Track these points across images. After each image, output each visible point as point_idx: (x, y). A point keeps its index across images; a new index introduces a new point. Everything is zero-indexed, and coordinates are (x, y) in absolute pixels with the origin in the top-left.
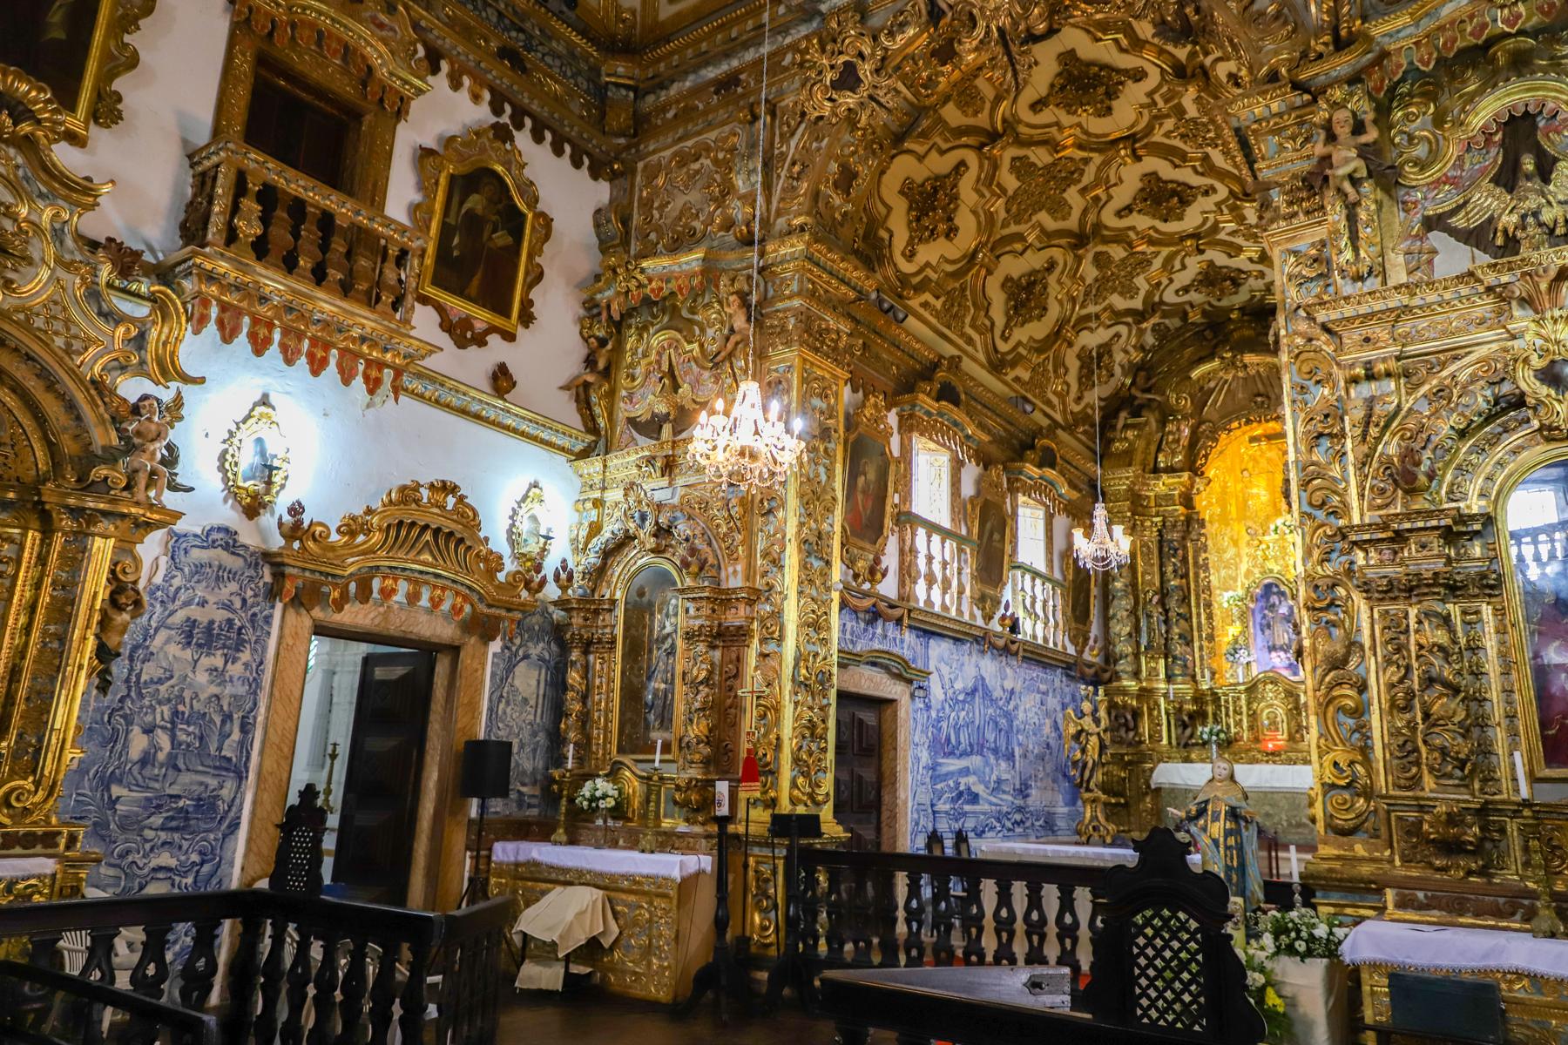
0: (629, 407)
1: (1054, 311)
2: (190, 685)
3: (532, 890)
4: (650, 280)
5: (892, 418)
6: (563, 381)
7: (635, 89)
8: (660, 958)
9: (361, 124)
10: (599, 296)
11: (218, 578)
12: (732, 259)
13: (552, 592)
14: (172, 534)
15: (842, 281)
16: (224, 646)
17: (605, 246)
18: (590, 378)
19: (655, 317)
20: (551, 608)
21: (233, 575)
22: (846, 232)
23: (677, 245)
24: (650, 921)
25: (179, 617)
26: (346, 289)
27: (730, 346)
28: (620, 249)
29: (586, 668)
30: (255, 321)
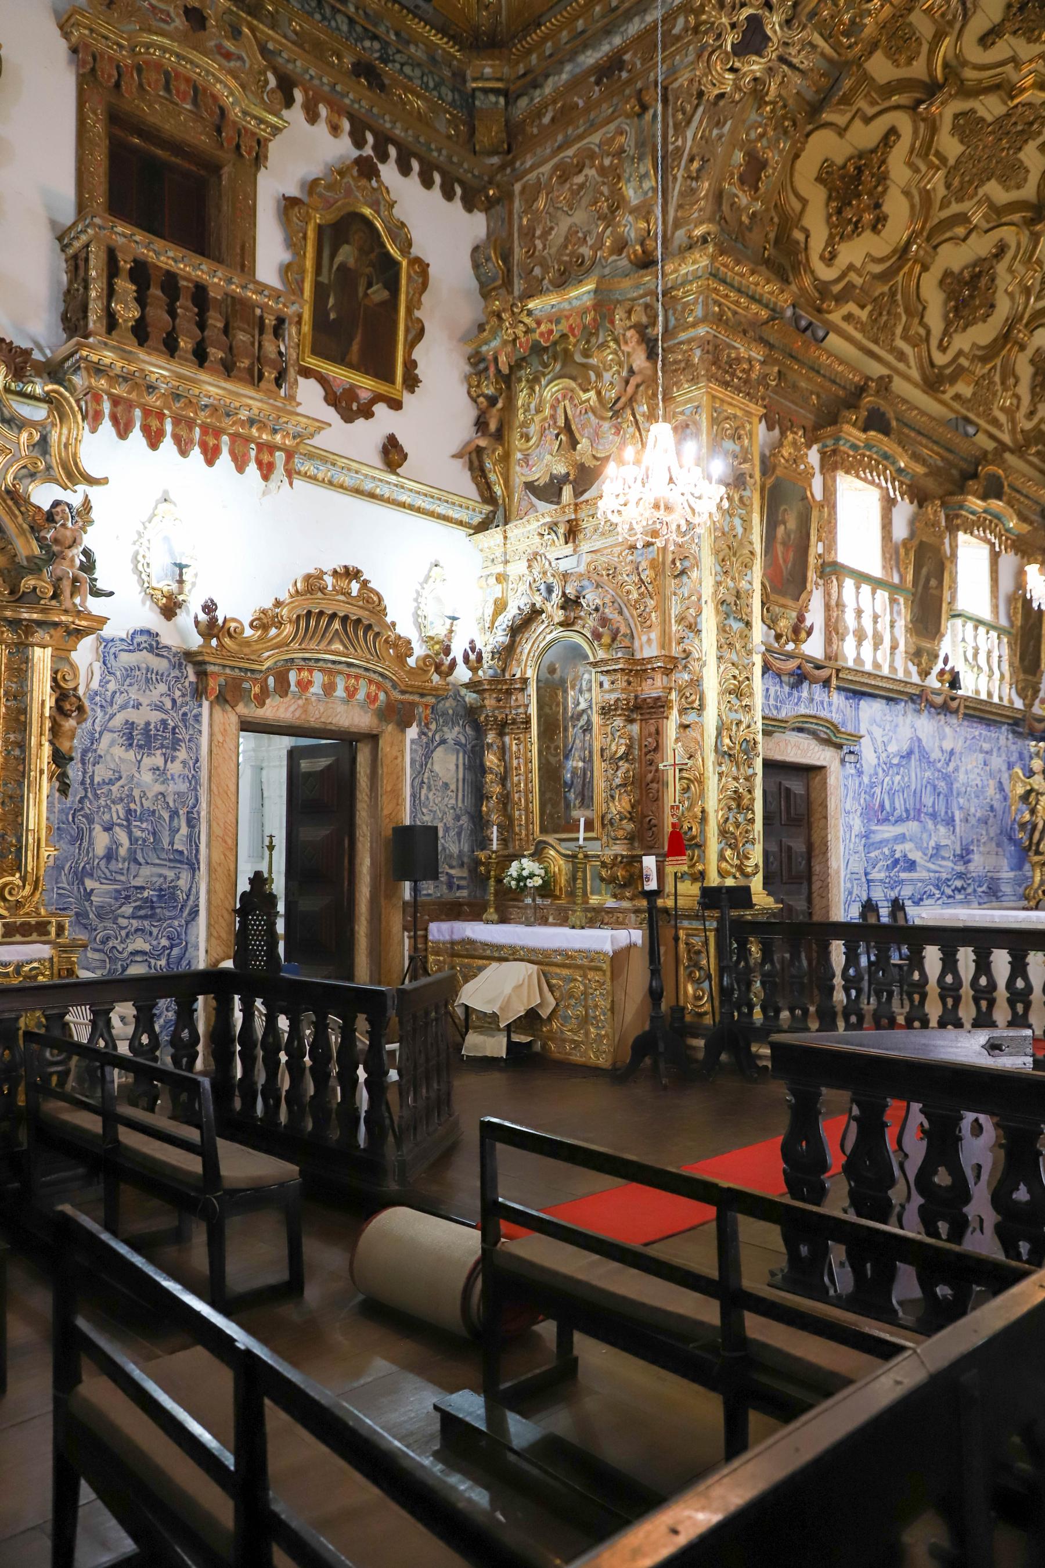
0: (525, 470)
1: (1003, 308)
2: (138, 785)
3: (469, 966)
4: (539, 323)
5: (813, 456)
6: (455, 448)
7: (505, 93)
8: (598, 1027)
9: (220, 177)
10: (484, 348)
11: (147, 681)
12: (627, 287)
13: (462, 674)
14: (101, 640)
15: (753, 298)
16: (162, 746)
17: (486, 292)
18: (483, 443)
19: (546, 366)
20: (463, 691)
21: (161, 677)
22: (755, 237)
23: (564, 280)
24: (584, 993)
25: (118, 721)
26: (228, 369)
27: (630, 389)
28: (503, 291)
29: (503, 750)
30: (147, 413)
